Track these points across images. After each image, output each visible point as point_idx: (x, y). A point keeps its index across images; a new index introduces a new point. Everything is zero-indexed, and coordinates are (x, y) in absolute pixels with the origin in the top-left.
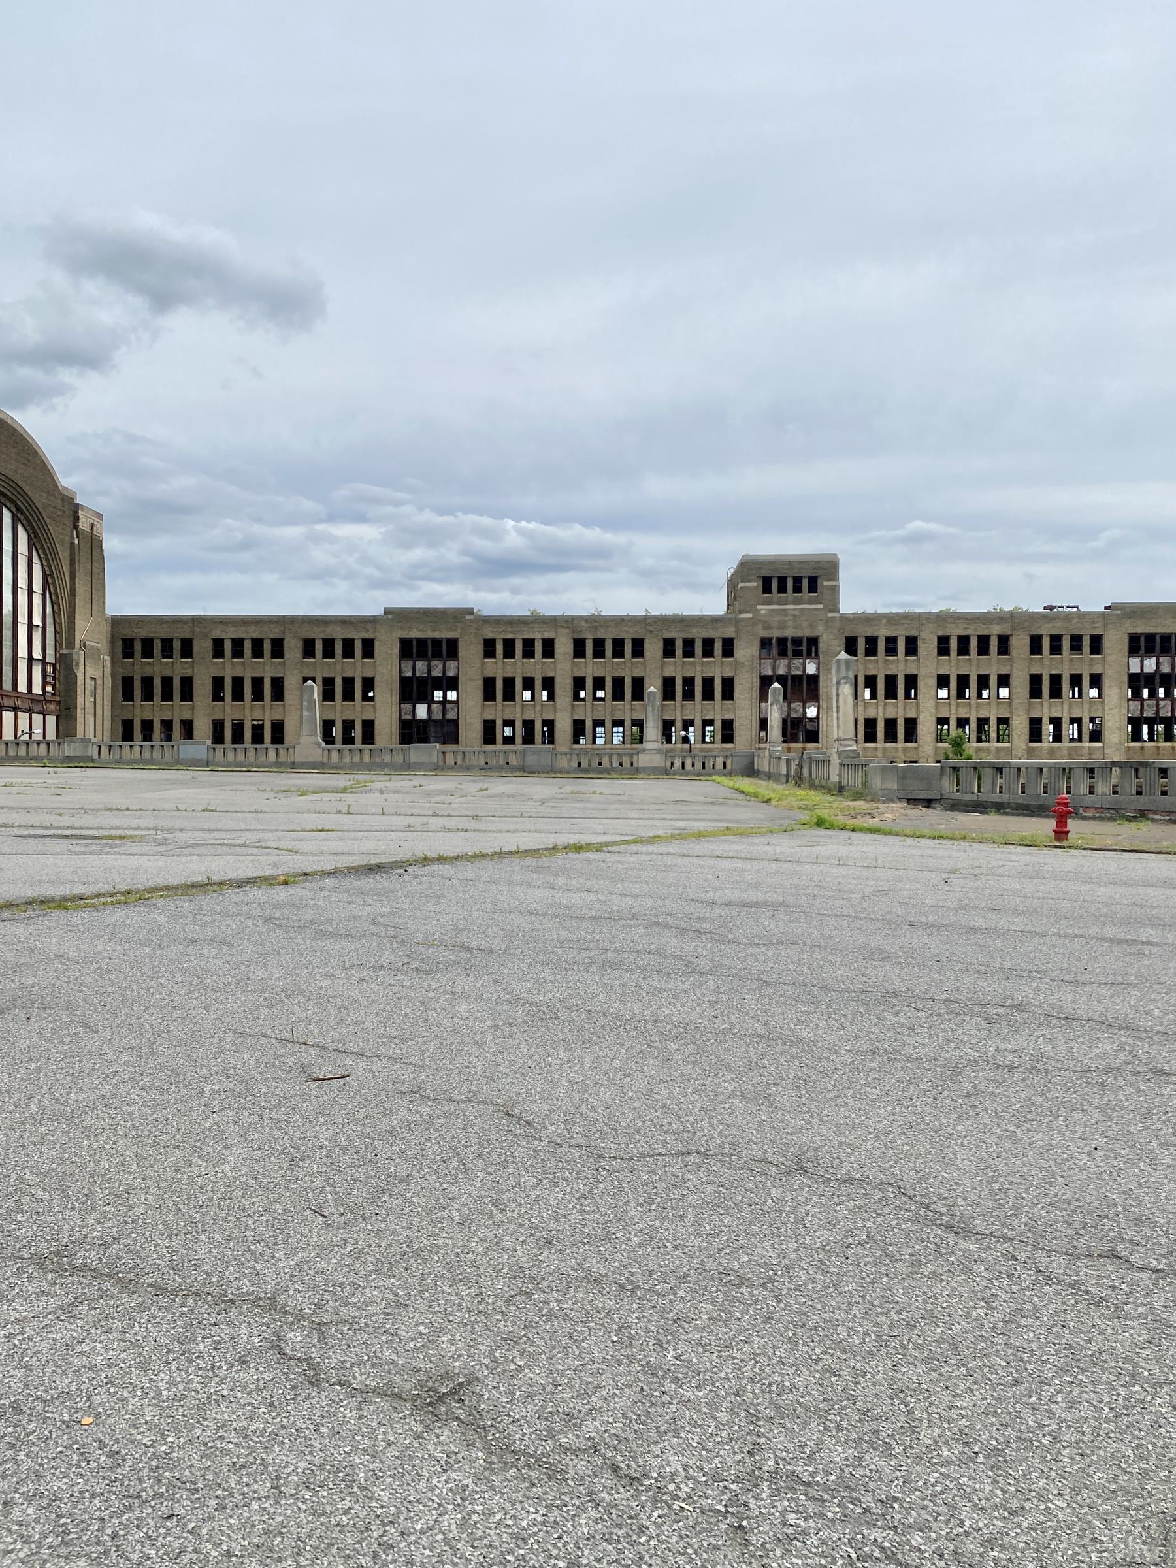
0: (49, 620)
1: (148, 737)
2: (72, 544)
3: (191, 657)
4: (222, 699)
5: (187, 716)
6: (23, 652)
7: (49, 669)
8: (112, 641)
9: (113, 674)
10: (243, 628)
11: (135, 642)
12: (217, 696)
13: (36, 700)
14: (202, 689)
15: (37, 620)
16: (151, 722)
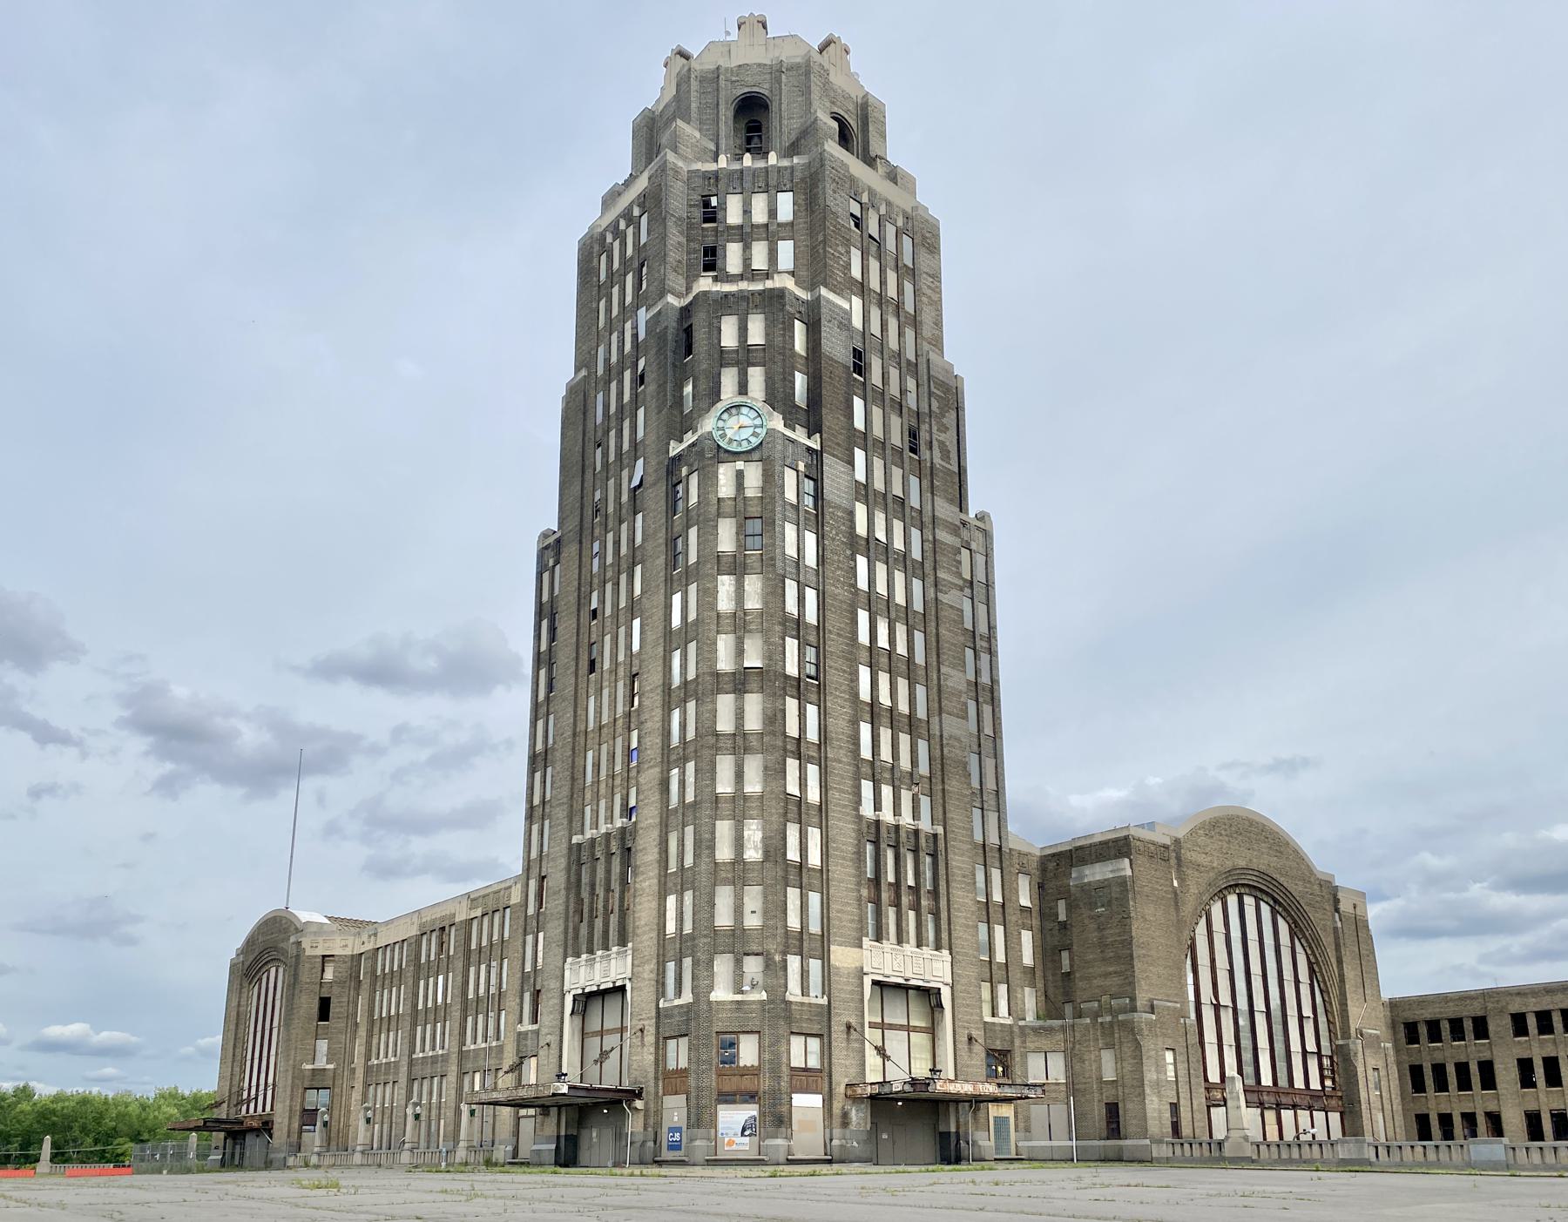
0: (1320, 1010)
1: (1448, 1135)
2: (1335, 929)
3: (1486, 1037)
4: (1534, 1085)
5: (1492, 1107)
7: (1326, 1062)
8: (1393, 1026)
9: (1399, 1063)
10: (1548, 998)
11: (1417, 1026)
12: (1527, 1081)
13: (1315, 1096)
14: (1507, 1074)
15: (1307, 1012)
16: (1450, 1116)
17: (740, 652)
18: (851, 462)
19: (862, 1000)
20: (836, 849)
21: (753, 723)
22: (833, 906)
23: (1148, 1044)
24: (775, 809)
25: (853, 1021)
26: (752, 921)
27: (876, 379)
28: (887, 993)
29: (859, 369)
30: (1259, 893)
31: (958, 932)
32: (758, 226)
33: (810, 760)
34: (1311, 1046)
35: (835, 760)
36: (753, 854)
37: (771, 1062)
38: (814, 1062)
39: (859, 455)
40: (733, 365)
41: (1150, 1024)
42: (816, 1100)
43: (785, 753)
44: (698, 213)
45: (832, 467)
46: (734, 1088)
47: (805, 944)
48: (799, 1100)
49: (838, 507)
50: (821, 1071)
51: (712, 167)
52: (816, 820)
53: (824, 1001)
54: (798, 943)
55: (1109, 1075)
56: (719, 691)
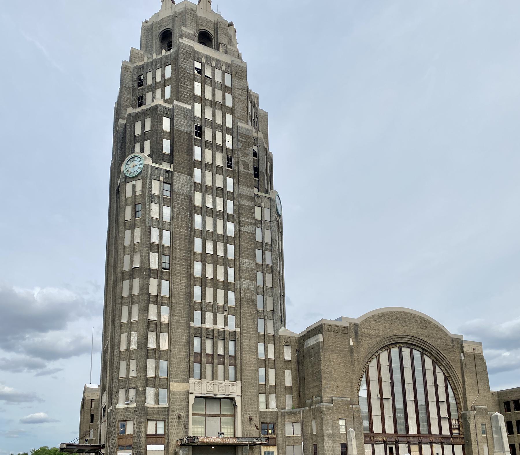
6: (433, 414)
17: (132, 262)
18: (191, 174)
19: (188, 405)
20: (174, 341)
21: (136, 291)
22: (173, 366)
23: (328, 418)
24: (142, 326)
25: (182, 413)
26: (133, 374)
27: (208, 136)
28: (207, 401)
29: (198, 134)
30: (408, 345)
31: (246, 372)
32: (158, 83)
33: (162, 304)
34: (444, 414)
35: (176, 303)
36: (133, 347)
37: (137, 432)
38: (161, 431)
39: (198, 172)
40: (139, 142)
41: (329, 409)
42: (162, 447)
43: (149, 302)
44: (136, 84)
45: (180, 179)
46: (124, 444)
47: (157, 383)
48: (150, 447)
49: (182, 194)
50: (164, 435)
51: (142, 63)
52: (166, 330)
53: (167, 406)
54: (156, 383)
55: (314, 433)
56: (123, 279)
